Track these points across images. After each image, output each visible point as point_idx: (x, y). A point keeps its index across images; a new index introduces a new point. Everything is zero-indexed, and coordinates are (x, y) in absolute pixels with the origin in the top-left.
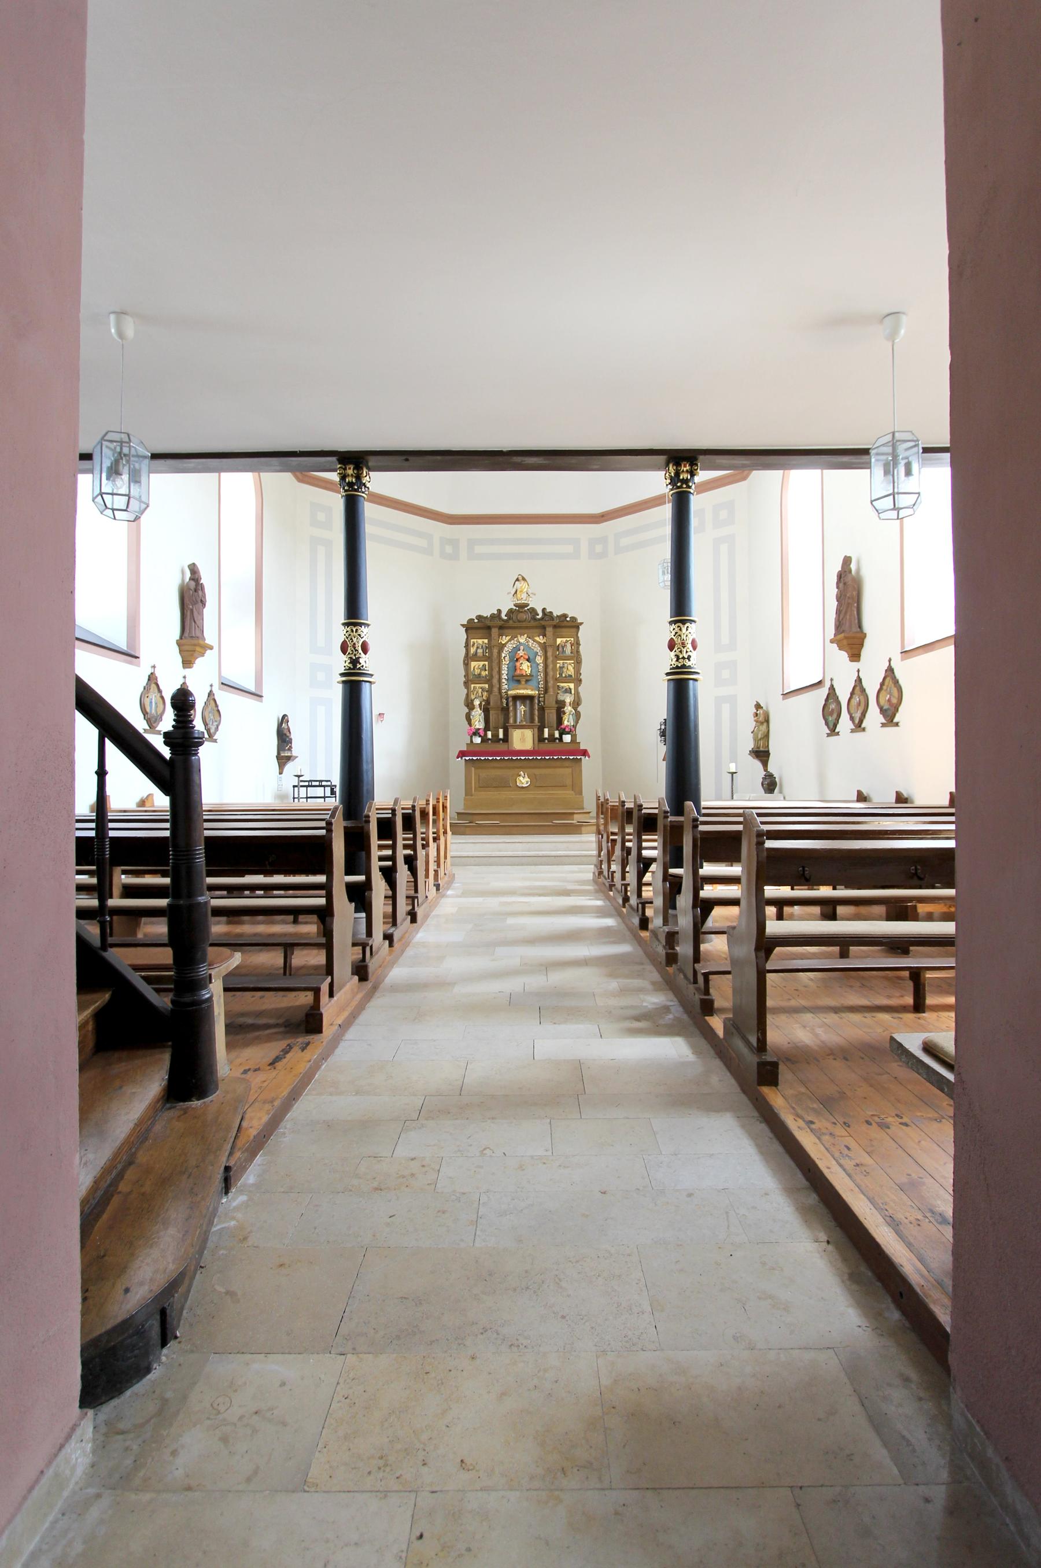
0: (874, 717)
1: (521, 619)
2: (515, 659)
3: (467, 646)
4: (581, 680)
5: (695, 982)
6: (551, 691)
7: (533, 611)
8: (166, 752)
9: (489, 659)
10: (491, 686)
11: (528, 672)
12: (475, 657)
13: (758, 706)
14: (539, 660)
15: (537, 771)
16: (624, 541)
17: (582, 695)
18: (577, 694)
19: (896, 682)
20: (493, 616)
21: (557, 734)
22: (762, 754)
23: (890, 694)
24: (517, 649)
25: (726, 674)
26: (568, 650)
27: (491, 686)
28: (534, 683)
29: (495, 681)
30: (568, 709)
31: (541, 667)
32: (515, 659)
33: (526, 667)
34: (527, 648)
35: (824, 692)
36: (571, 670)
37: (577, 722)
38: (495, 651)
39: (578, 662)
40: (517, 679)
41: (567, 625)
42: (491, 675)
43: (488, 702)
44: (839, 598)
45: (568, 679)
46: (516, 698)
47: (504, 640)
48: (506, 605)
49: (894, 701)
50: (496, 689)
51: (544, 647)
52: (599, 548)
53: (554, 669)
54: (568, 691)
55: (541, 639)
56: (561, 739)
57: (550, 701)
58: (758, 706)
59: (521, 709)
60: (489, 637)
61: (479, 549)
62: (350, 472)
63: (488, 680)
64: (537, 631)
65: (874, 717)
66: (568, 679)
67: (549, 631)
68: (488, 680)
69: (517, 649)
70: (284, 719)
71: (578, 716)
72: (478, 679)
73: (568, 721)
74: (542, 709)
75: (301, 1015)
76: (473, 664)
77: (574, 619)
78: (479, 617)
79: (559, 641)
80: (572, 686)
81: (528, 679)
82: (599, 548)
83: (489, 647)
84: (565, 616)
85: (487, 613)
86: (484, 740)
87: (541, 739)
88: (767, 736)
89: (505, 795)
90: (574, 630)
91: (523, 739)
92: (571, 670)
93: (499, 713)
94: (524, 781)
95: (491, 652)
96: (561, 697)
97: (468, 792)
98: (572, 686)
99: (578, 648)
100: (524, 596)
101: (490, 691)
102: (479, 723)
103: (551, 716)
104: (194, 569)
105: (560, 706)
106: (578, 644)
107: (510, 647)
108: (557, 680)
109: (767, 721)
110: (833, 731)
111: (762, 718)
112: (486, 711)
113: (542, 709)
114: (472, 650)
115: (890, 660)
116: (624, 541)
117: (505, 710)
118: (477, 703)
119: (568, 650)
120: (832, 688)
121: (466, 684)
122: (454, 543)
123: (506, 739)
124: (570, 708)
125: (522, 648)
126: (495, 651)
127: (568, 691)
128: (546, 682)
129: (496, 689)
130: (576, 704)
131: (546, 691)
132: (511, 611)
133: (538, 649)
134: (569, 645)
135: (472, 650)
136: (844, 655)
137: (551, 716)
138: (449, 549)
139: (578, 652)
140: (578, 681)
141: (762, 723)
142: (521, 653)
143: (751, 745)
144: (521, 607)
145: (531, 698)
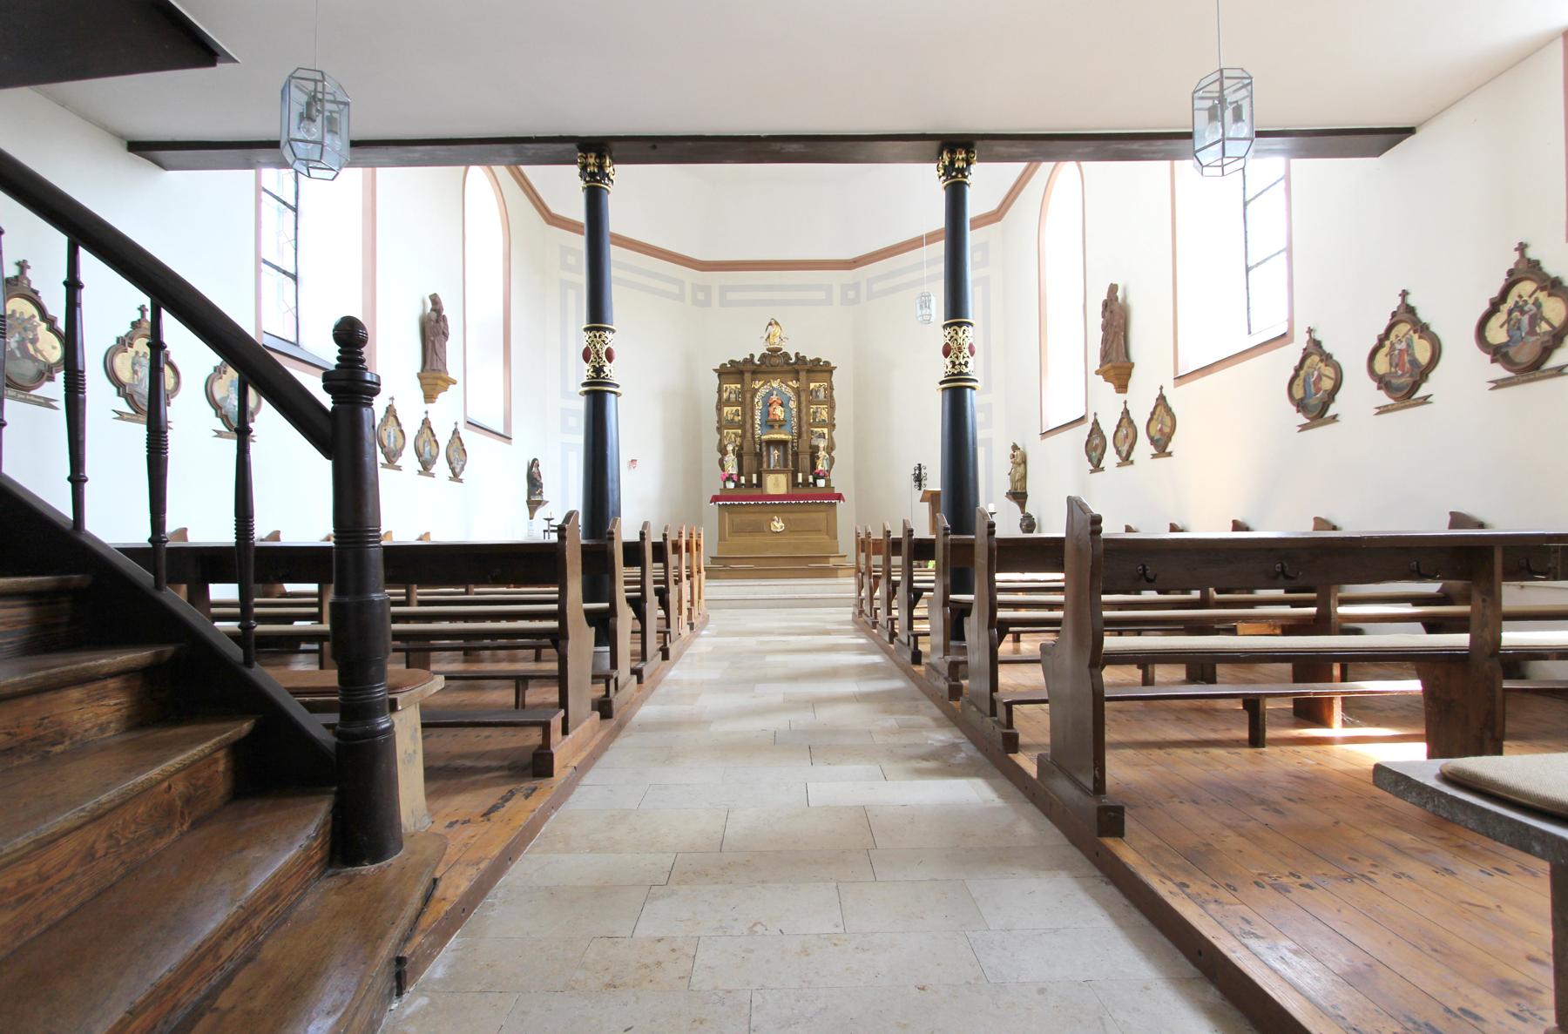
0: (1144, 447)
1: (774, 364)
2: (768, 404)
3: (720, 391)
5: (993, 713)
6: (805, 436)
7: (786, 355)
8: (326, 401)
9: (742, 404)
10: (744, 432)
12: (728, 403)
13: (1015, 448)
14: (793, 405)
15: (791, 516)
16: (877, 287)
19: (1168, 410)
20: (745, 360)
21: (811, 479)
23: (1162, 423)
24: (770, 394)
26: (822, 394)
27: (744, 432)
28: (787, 428)
29: (748, 426)
30: (822, 454)
31: (794, 412)
32: (768, 404)
33: (779, 412)
34: (780, 392)
35: (1086, 428)
36: (824, 415)
38: (748, 396)
39: (832, 407)
40: (770, 424)
41: (820, 369)
42: (744, 420)
43: (741, 447)
44: (1104, 328)
45: (822, 424)
46: (770, 443)
47: (757, 385)
48: (759, 350)
49: (1167, 430)
50: (749, 435)
51: (797, 392)
52: (851, 294)
53: (808, 413)
54: (822, 436)
55: (794, 384)
56: (815, 484)
57: (804, 446)
58: (1015, 448)
59: (775, 453)
60: (742, 382)
61: (731, 296)
62: (592, 161)
63: (742, 425)
64: (790, 376)
65: (1144, 447)
66: (822, 424)
67: (803, 375)
68: (742, 425)
69: (770, 394)
70: (534, 463)
71: (832, 461)
72: (731, 424)
73: (822, 466)
74: (796, 455)
75: (528, 758)
76: (726, 409)
77: (827, 363)
78: (732, 362)
79: (812, 385)
80: (825, 430)
81: (782, 424)
82: (851, 294)
83: (742, 392)
84: (818, 360)
85: (739, 358)
86: (738, 485)
87: (795, 484)
88: (1024, 477)
89: (759, 539)
91: (777, 485)
92: (824, 415)
93: (752, 458)
94: (778, 525)
95: (744, 398)
96: (814, 443)
97: (722, 538)
98: (825, 430)
100: (777, 340)
101: (743, 436)
102: (732, 468)
103: (805, 461)
104: (435, 299)
105: (814, 451)
106: (832, 388)
107: (763, 392)
108: (810, 425)
109: (1025, 462)
110: (1097, 467)
112: (740, 456)
113: (796, 455)
114: (725, 395)
116: (877, 287)
117: (759, 456)
118: (730, 448)
119: (822, 394)
120: (1096, 423)
121: (719, 430)
122: (706, 289)
123: (760, 484)
126: (748, 396)
127: (822, 436)
128: (800, 427)
129: (749, 435)
130: (830, 448)
131: (800, 435)
132: (763, 356)
133: (791, 394)
135: (725, 395)
136: (1110, 387)
137: (805, 461)
138: (701, 296)
140: (832, 426)
142: (774, 398)
143: (1008, 487)
144: (774, 351)
145: (784, 443)
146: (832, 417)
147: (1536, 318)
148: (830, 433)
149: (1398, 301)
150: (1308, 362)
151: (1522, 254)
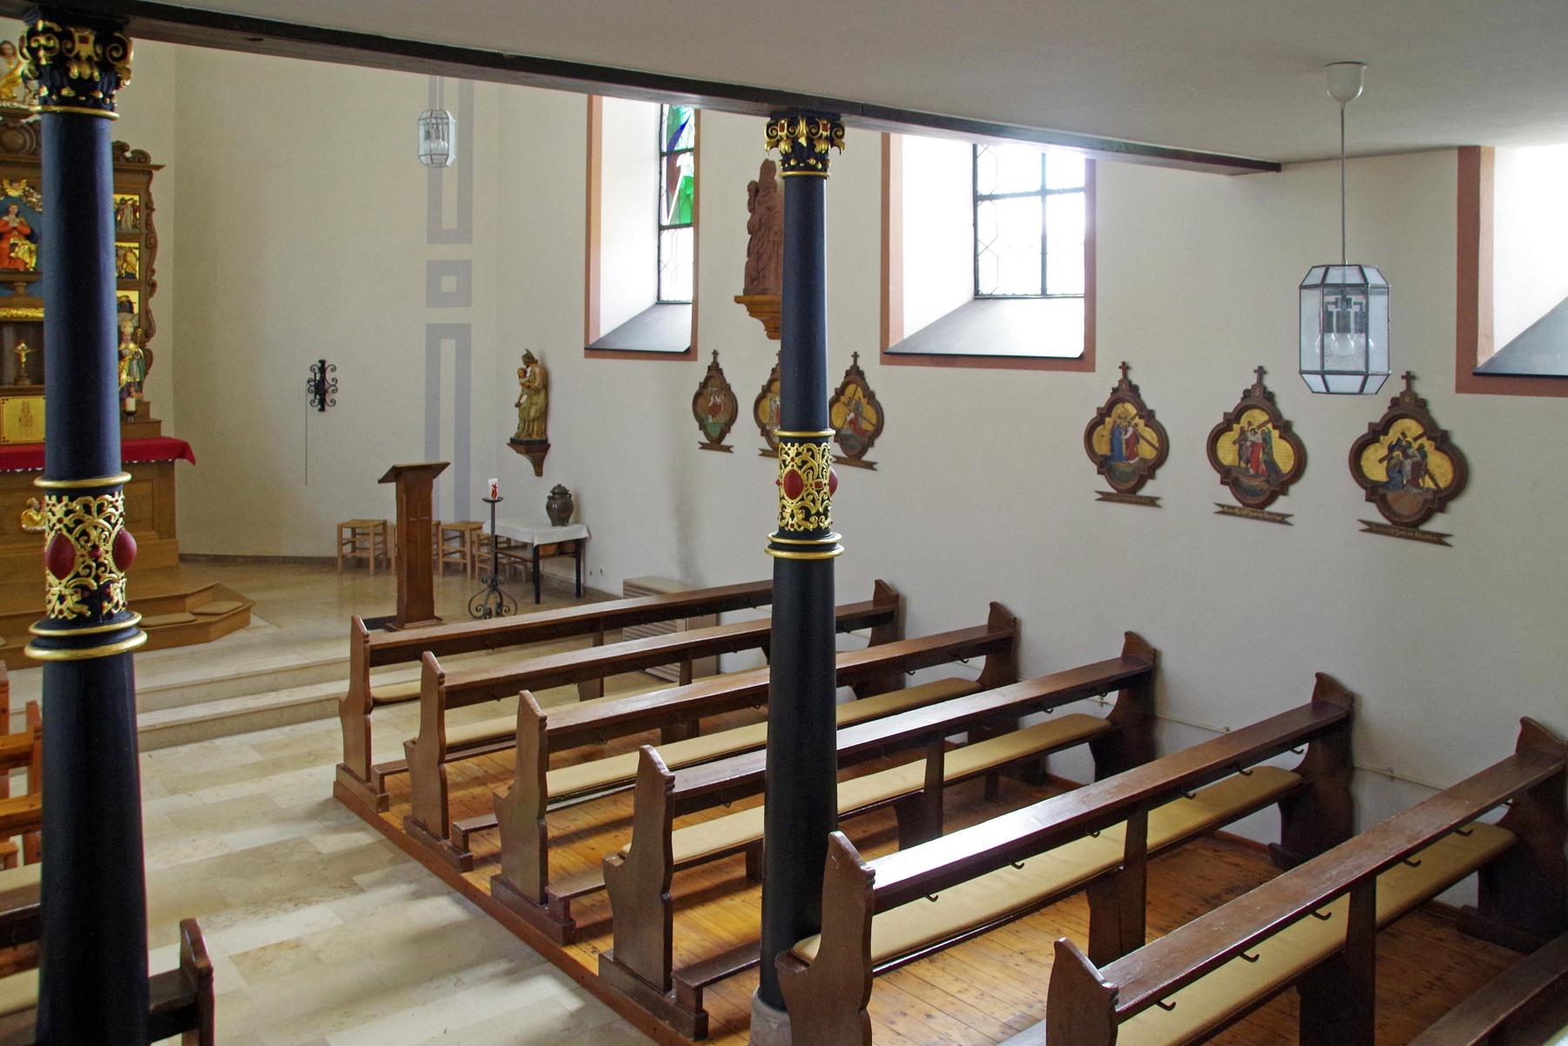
4: (153, 286)
11: (32, 262)
13: (529, 359)
17: (155, 315)
18: (146, 311)
22: (533, 446)
25: (449, 284)
35: (697, 372)
37: (146, 373)
39: (150, 246)
44: (752, 229)
58: (529, 359)
88: (544, 414)
90: (144, 178)
98: (134, 296)
99: (149, 216)
109: (546, 386)
110: (716, 443)
111: (536, 381)
115: (856, 356)
120: (715, 370)
124: (132, 346)
125: (14, 208)
134: (128, 211)
139: (149, 224)
140: (148, 287)
141: (537, 391)
143: (512, 427)
146: (149, 269)
147: (1421, 468)
148: (144, 301)
149: (1253, 379)
150: (1119, 409)
151: (1409, 386)
